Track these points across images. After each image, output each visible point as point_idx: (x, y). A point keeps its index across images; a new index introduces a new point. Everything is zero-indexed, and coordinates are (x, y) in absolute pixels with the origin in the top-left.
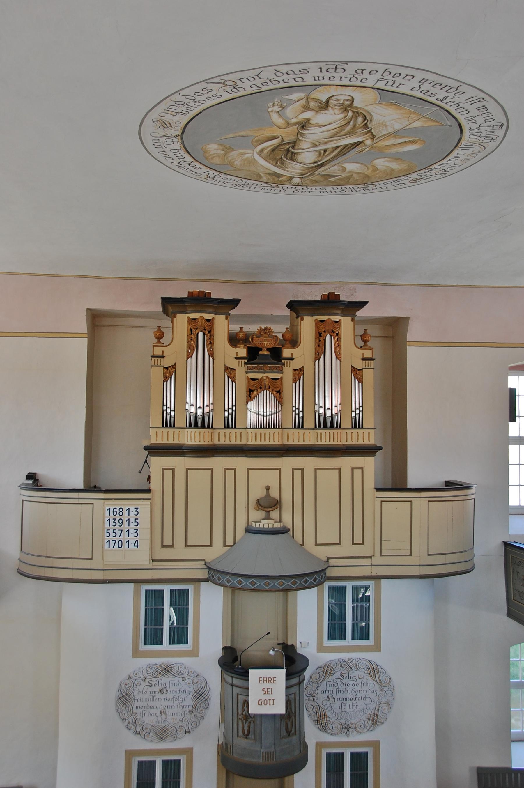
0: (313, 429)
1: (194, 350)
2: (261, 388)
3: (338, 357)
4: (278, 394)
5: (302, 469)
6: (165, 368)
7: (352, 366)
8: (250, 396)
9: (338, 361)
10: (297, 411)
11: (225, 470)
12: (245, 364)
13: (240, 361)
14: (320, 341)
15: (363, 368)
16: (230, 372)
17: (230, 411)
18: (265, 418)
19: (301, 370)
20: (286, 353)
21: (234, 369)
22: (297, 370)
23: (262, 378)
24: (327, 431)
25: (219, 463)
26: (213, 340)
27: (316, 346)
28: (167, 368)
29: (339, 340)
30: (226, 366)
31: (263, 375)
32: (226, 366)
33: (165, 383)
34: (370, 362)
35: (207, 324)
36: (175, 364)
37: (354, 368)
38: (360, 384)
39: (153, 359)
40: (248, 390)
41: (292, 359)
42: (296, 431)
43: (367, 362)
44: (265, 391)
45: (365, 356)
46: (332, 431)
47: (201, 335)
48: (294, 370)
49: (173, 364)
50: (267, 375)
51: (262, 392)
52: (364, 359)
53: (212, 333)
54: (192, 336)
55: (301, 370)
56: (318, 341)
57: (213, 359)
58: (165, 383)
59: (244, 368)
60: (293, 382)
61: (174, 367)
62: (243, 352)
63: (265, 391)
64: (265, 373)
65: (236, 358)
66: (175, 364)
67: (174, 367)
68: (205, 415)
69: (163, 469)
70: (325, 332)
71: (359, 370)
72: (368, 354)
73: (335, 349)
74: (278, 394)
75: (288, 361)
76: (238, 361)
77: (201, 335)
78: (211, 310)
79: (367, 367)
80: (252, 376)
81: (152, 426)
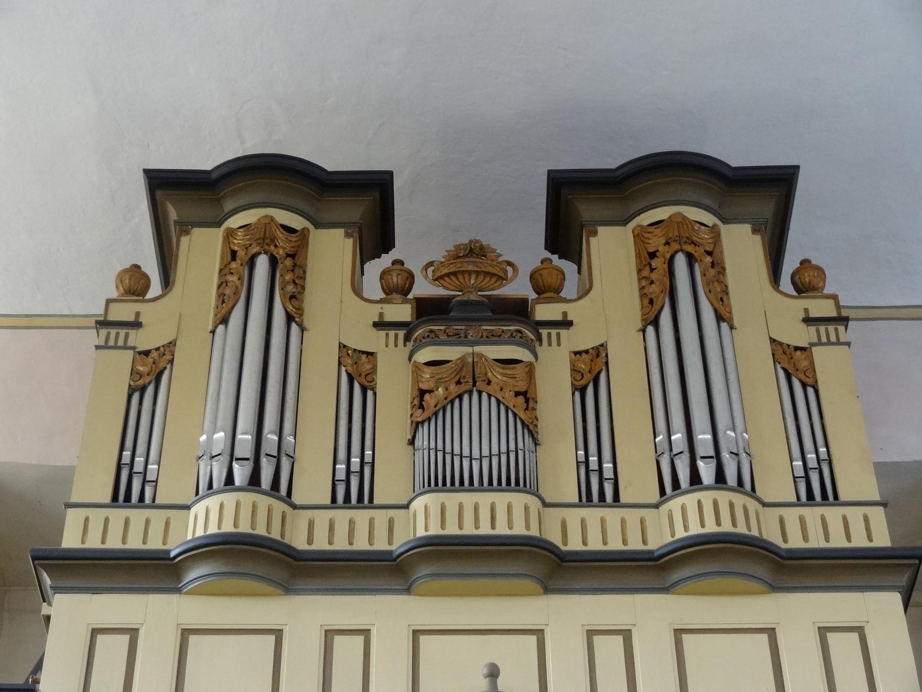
0: (656, 506)
1: (236, 293)
2: (458, 383)
3: (722, 310)
4: (521, 399)
5: (627, 635)
6: (140, 353)
7: (773, 341)
8: (421, 407)
9: (724, 326)
10: (593, 459)
11: (329, 635)
12: (407, 339)
13: (392, 333)
14: (652, 270)
15: (812, 345)
16: (358, 371)
17: (355, 461)
18: (476, 465)
19: (599, 352)
20: (544, 312)
21: (372, 354)
22: (587, 352)
23: (463, 359)
24: (706, 497)
25: (307, 616)
26: (303, 278)
27: (642, 288)
28: (147, 353)
29: (718, 266)
30: (342, 347)
31: (469, 350)
32: (342, 347)
33: (136, 397)
34: (831, 328)
35: (280, 234)
36: (172, 344)
37: (781, 344)
38: (810, 391)
39: (103, 332)
40: (416, 393)
41: (566, 324)
42: (593, 515)
43: (822, 329)
44: (475, 396)
45: (813, 314)
46: (723, 497)
47: (262, 263)
48: (576, 353)
49: (165, 342)
50: (478, 349)
51: (466, 398)
52: (808, 320)
53: (299, 261)
54: (233, 265)
55: (599, 352)
56: (646, 272)
57: (303, 329)
58: (136, 397)
59: (403, 351)
60: (575, 388)
61: (168, 349)
62: (402, 312)
63: (475, 396)
64: (472, 344)
65: (380, 325)
66: (172, 344)
67: (168, 349)
68: (264, 461)
69: (95, 632)
70: (667, 243)
71: (797, 349)
72: (821, 308)
73: (707, 284)
74: (521, 399)
75: (554, 332)
76: (382, 334)
77: (262, 263)
78: (301, 205)
79: (824, 339)
80: (426, 355)
81: (74, 499)
